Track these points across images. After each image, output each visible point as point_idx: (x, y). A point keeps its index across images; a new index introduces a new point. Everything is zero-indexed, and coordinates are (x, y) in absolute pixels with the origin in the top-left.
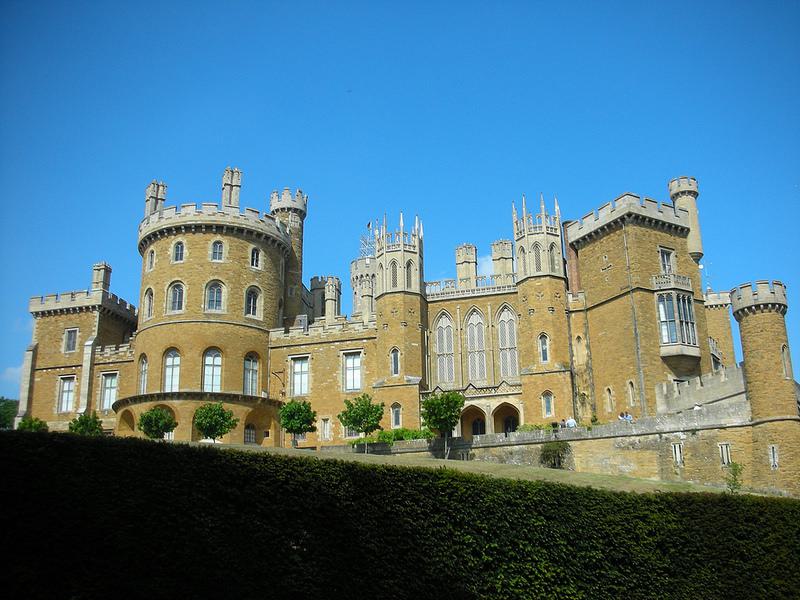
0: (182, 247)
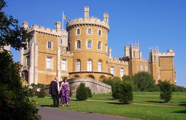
0: (79, 30)
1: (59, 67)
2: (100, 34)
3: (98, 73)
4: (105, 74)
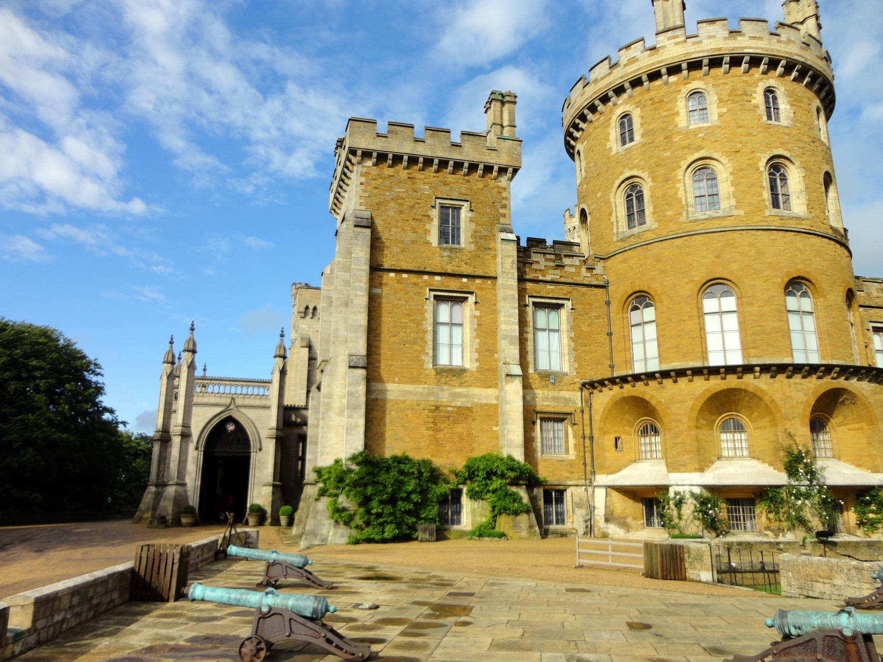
2: (771, 108)
3: (797, 369)
4: (854, 381)
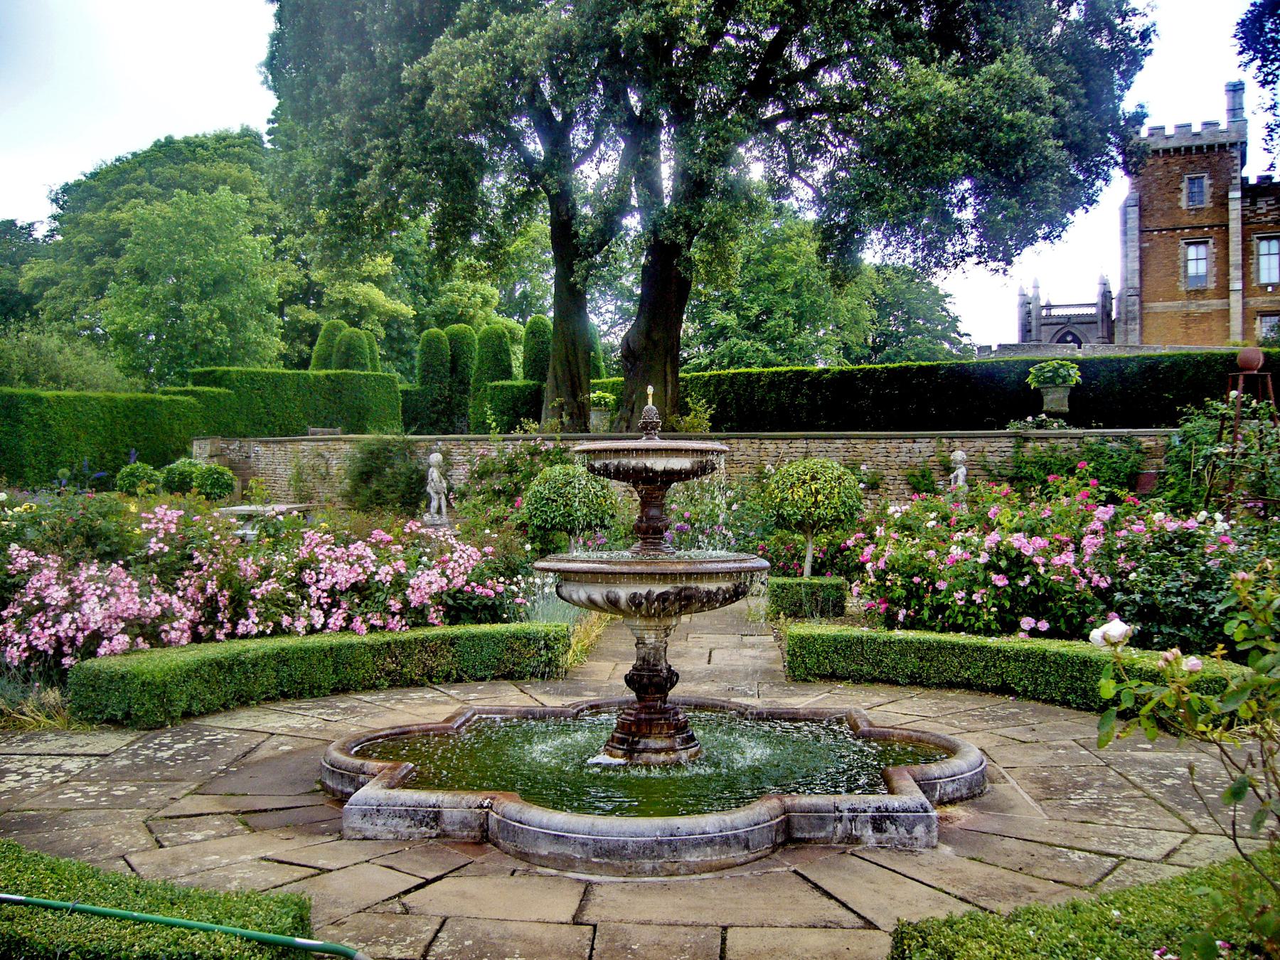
1: (1236, 274)
